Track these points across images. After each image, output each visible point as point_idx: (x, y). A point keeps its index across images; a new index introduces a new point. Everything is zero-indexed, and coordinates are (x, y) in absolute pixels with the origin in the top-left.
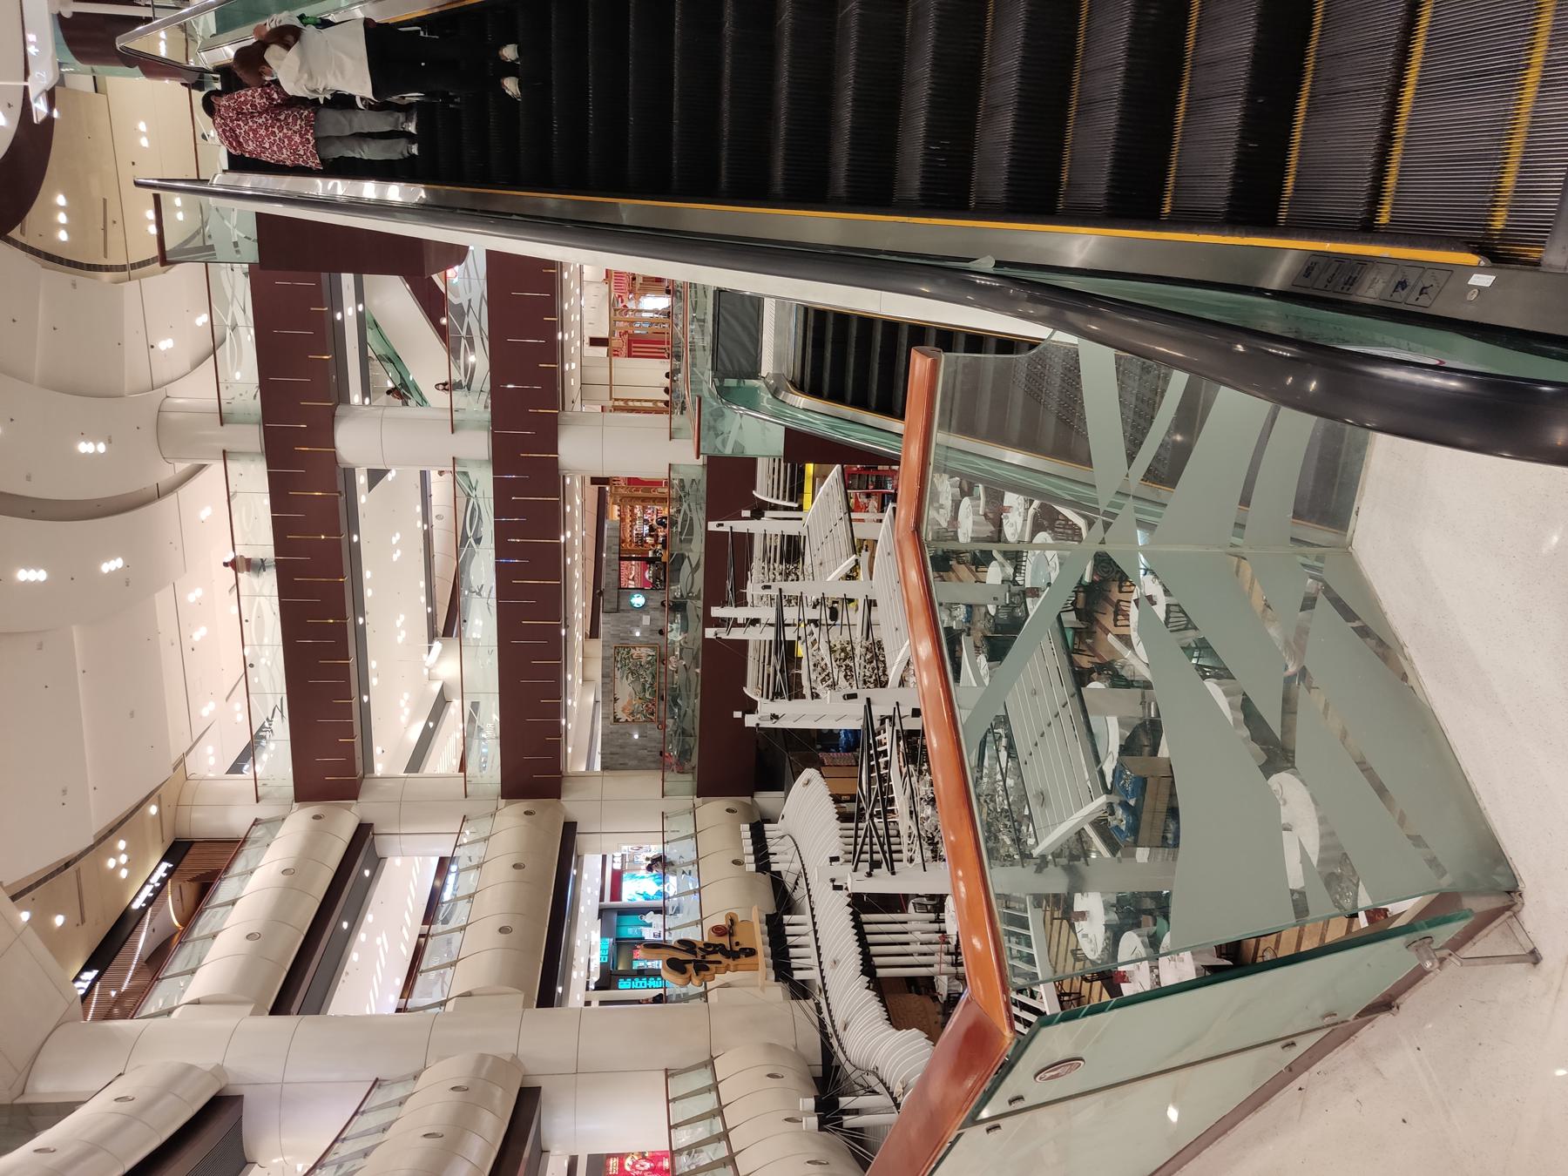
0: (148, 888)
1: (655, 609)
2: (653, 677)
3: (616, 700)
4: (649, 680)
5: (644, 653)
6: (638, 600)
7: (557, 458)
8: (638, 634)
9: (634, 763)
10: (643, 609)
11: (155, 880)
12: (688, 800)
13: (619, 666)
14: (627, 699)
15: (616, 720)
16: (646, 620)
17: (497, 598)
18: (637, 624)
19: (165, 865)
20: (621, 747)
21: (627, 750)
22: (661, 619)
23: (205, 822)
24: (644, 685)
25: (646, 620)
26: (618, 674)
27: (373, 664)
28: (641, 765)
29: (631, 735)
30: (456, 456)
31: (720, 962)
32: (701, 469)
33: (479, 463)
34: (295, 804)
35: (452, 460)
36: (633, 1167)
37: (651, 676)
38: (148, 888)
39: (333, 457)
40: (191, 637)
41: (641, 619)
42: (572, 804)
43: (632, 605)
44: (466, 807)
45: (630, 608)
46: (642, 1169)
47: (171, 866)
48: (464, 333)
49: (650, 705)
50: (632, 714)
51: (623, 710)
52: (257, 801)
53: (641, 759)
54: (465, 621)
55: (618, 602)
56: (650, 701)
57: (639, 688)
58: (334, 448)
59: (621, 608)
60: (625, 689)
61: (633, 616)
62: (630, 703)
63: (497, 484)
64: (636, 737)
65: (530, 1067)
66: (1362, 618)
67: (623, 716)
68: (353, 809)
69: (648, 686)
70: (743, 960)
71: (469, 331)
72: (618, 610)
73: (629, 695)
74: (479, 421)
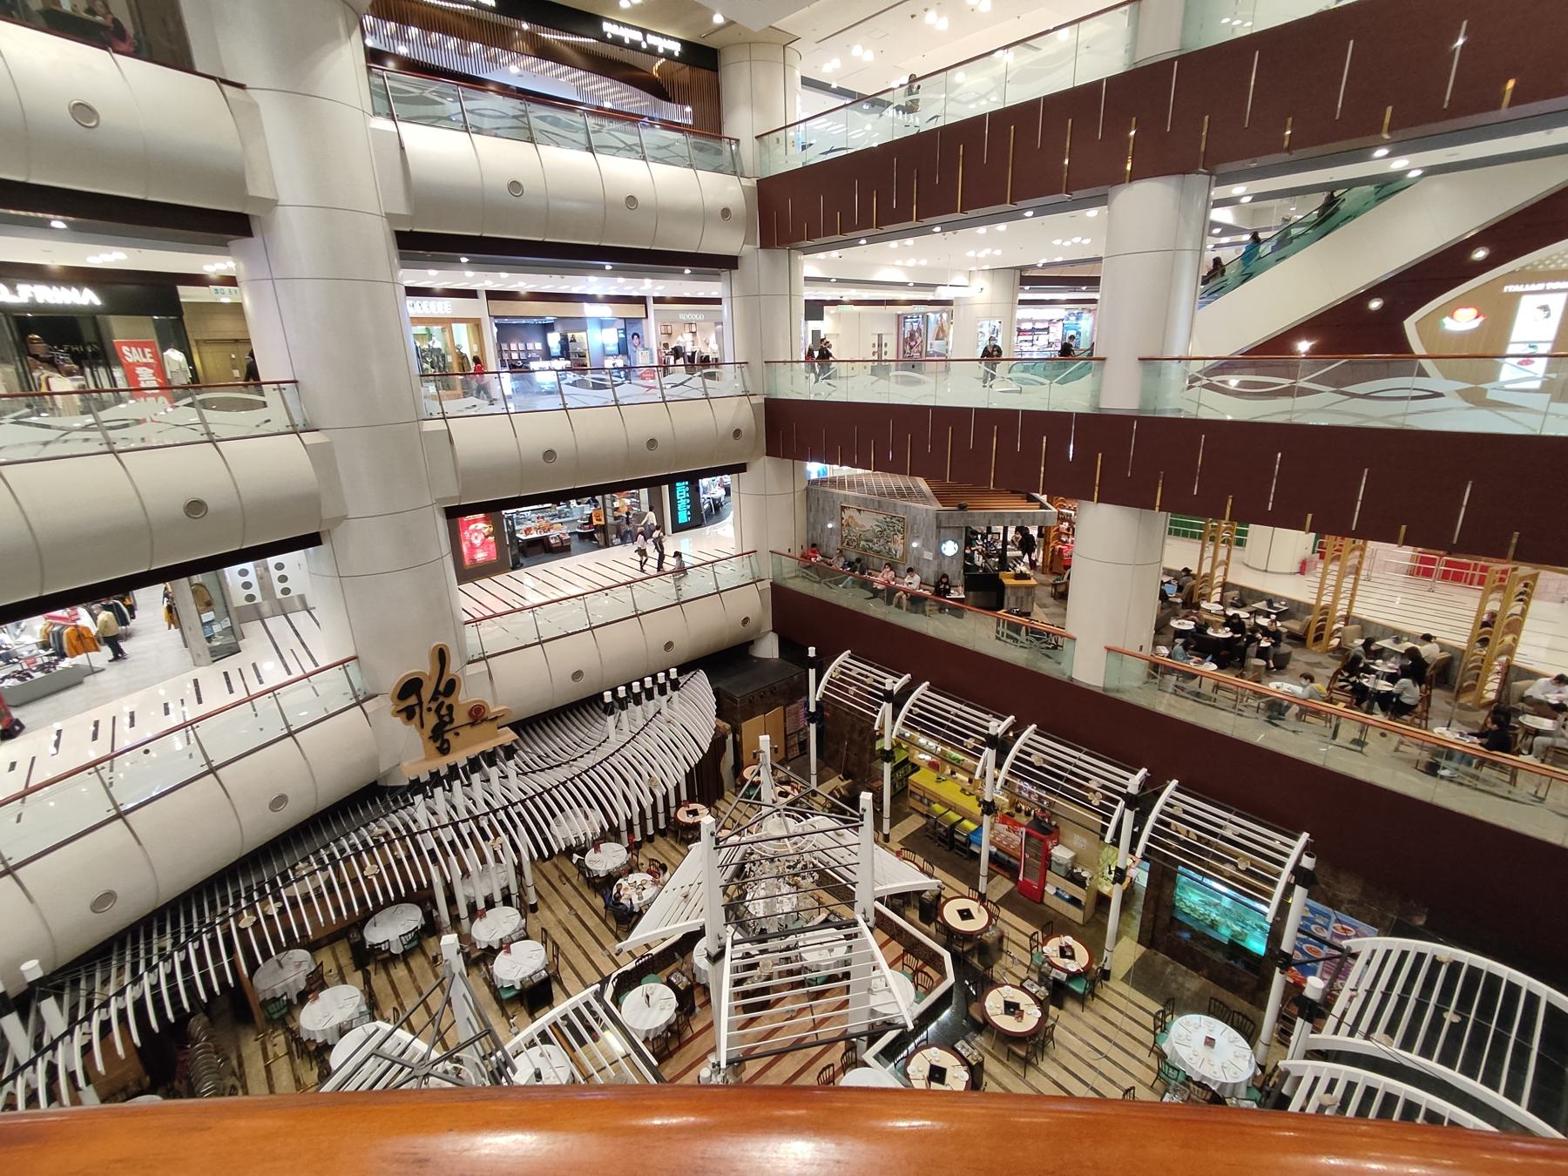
0: (638, 36)
1: (940, 565)
2: (878, 552)
3: (859, 511)
4: (875, 547)
5: (898, 547)
6: (950, 548)
7: (1093, 500)
8: (915, 545)
9: (812, 520)
10: (939, 554)
11: (652, 39)
12: (768, 576)
13: (888, 520)
14: (860, 523)
15: (843, 508)
16: (928, 555)
17: (935, 407)
18: (925, 545)
19: (676, 48)
20: (823, 509)
21: (821, 514)
22: (930, 573)
23: (737, 79)
24: (871, 541)
25: (928, 555)
26: (881, 517)
27: (909, 242)
28: (813, 524)
29: (831, 520)
30: (1107, 362)
31: (422, 726)
32: (1068, 674)
33: (1096, 395)
34: (755, 180)
35: (1102, 357)
36: (476, 531)
37: (878, 549)
38: (638, 36)
39: (1119, 179)
40: (926, 10)
41: (929, 550)
42: (764, 468)
43: (945, 542)
44: (757, 363)
45: (942, 539)
46: (473, 538)
47: (677, 54)
48: (1302, 383)
49: (855, 544)
50: (848, 525)
51: (851, 517)
52: (757, 137)
53: (814, 529)
54: (913, 367)
55: (950, 527)
56: (858, 545)
57: (869, 535)
58: (1130, 181)
59: (942, 530)
60: (867, 522)
61: (933, 541)
62: (856, 524)
63: (1064, 418)
64: (830, 526)
65: (337, 533)
66: (1065, 904)
67: (846, 515)
68: (748, 248)
69: (871, 544)
70: (433, 746)
71: (1304, 392)
72: (939, 527)
73: (863, 526)
74: (1156, 398)
